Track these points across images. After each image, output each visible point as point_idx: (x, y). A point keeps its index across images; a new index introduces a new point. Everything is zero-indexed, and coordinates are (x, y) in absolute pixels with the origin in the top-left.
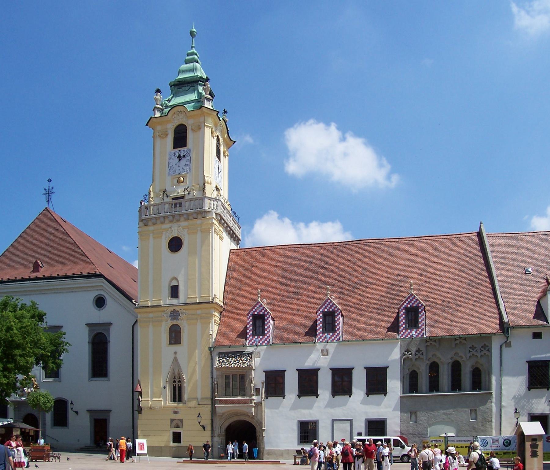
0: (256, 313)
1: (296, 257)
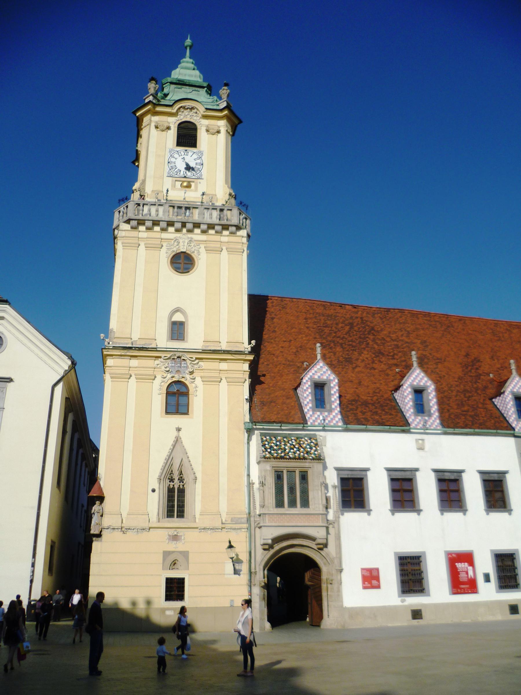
0: (316, 377)
1: (328, 316)
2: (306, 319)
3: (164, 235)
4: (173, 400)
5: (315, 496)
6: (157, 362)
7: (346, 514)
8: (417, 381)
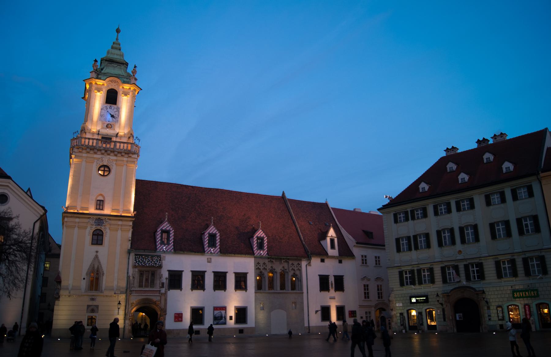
3: (95, 156)
4: (95, 237)
5: (157, 283)
6: (88, 220)
7: (171, 290)
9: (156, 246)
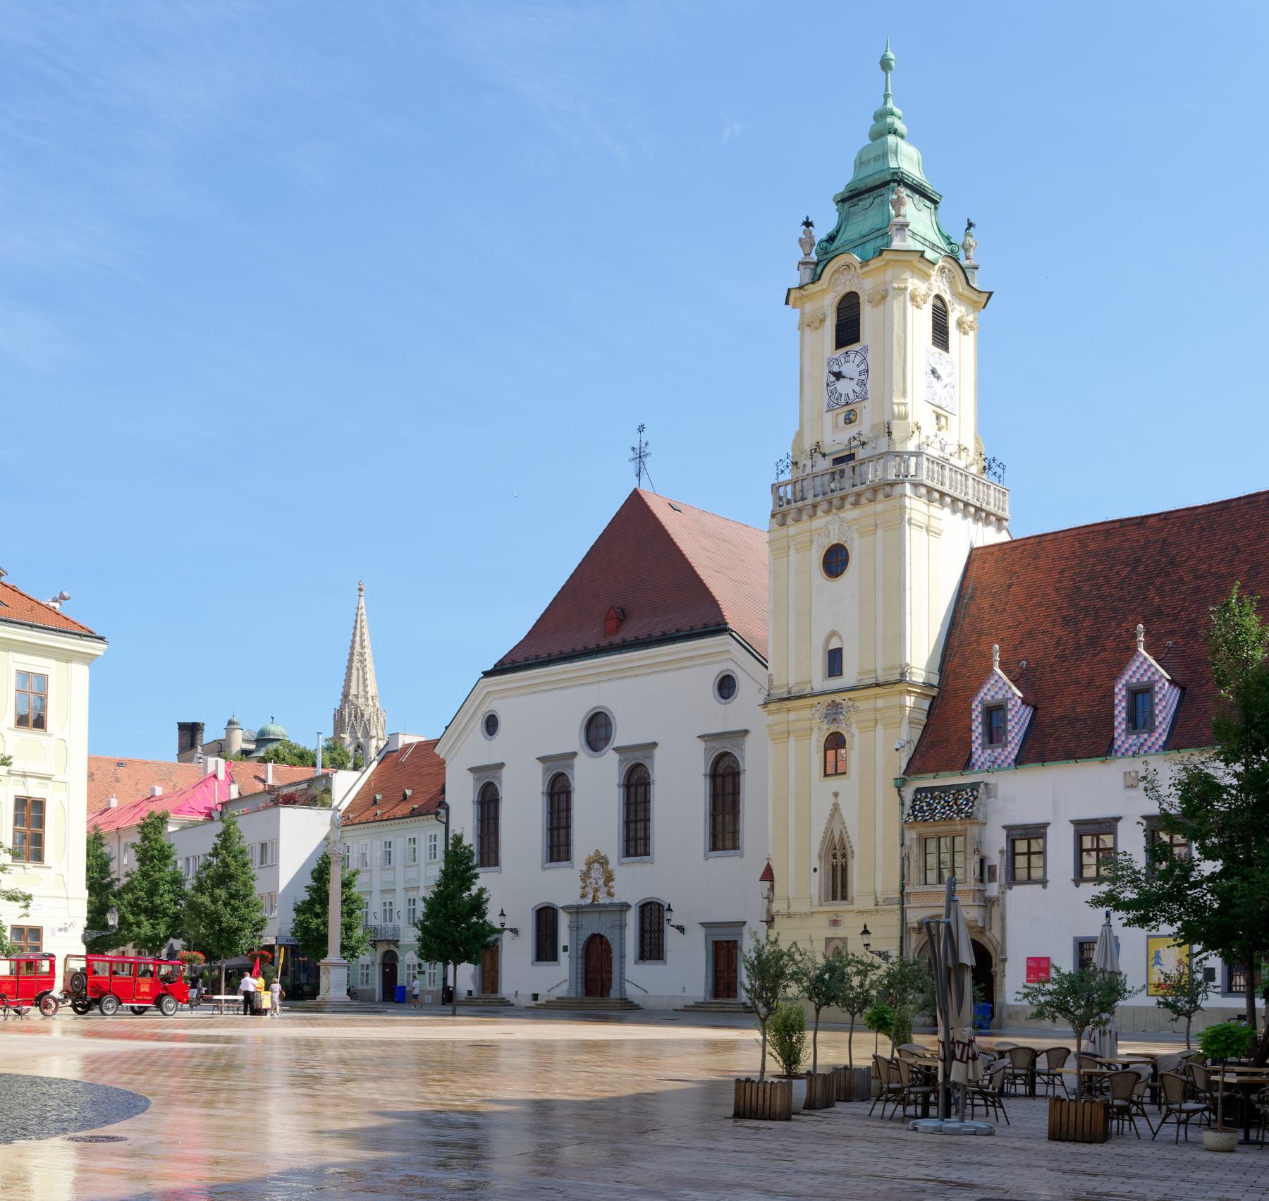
0: (989, 698)
2: (1062, 572)
8: (1138, 676)
9: (971, 753)
